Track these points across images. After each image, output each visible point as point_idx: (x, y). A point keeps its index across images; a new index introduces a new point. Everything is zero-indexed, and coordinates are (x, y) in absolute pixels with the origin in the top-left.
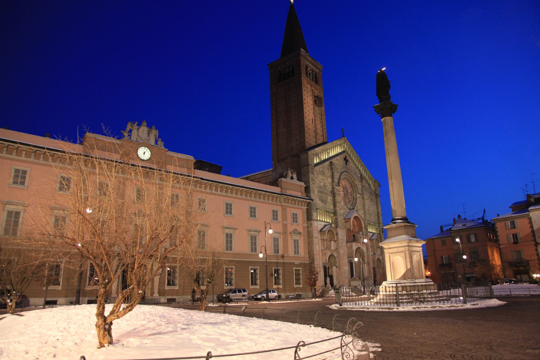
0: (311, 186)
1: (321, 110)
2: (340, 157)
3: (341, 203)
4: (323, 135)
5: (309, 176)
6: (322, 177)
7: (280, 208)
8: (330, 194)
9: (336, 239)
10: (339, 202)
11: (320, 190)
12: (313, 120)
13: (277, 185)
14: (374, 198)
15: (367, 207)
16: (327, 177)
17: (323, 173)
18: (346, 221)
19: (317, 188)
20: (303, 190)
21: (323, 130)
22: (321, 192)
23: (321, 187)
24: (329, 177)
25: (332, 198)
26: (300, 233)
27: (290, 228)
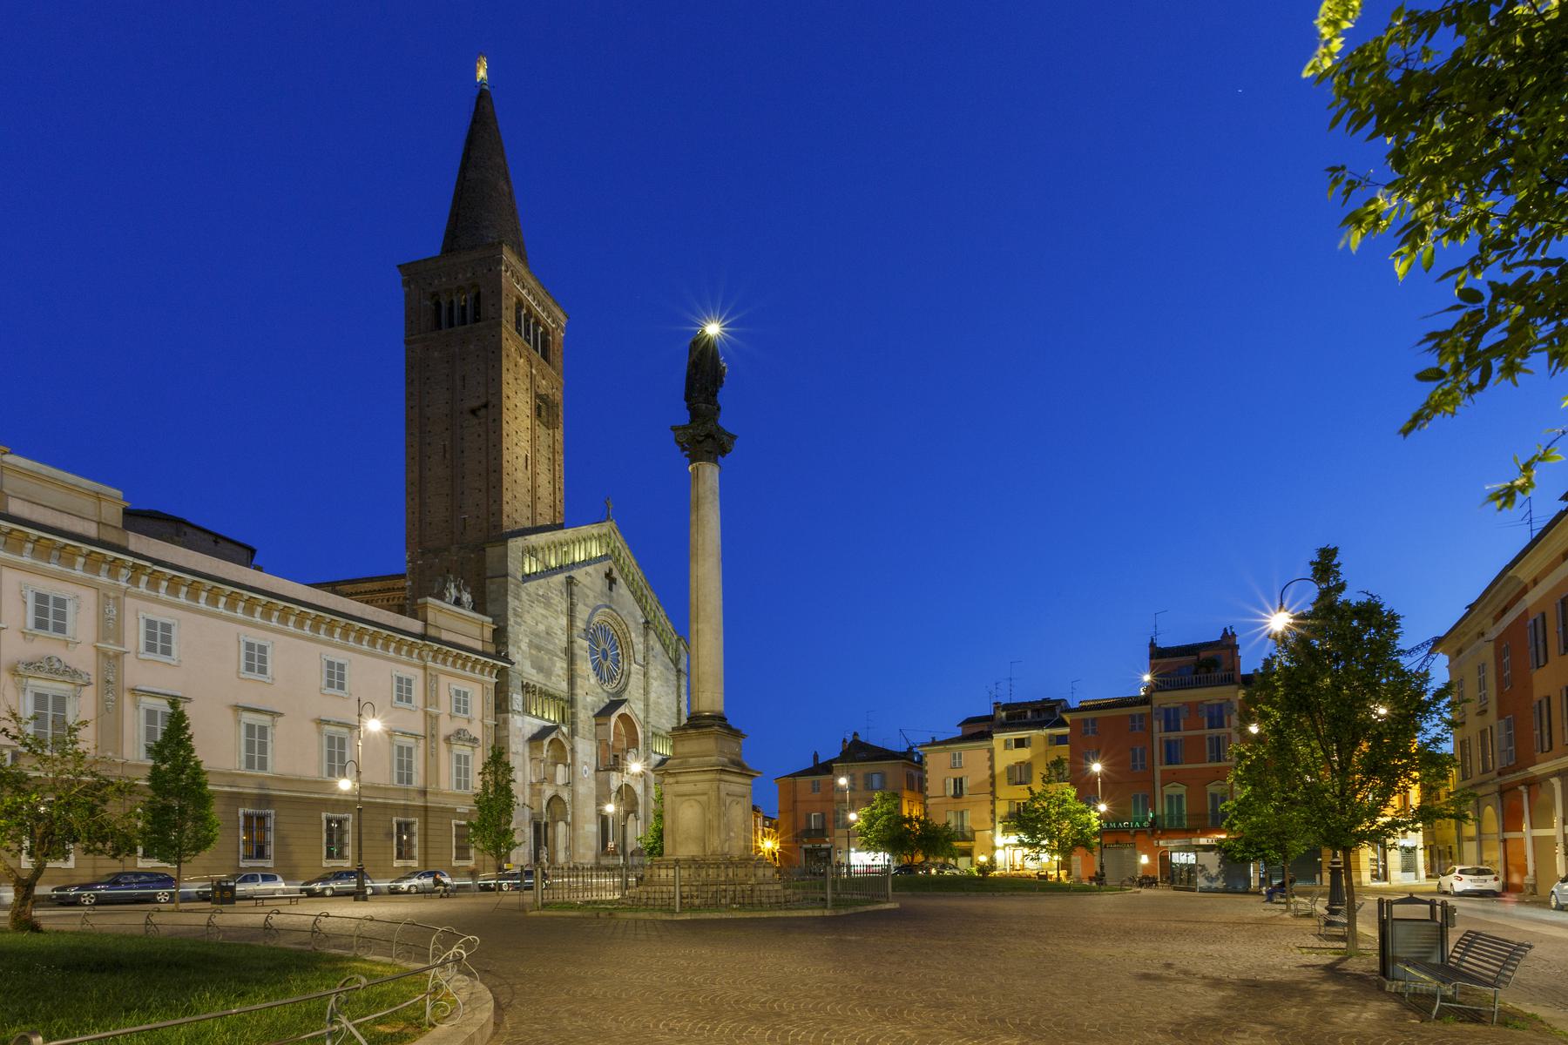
0: (509, 628)
2: (595, 569)
5: (507, 603)
6: (544, 612)
7: (420, 673)
8: (563, 655)
9: (569, 761)
10: (583, 677)
11: (536, 641)
14: (673, 677)
15: (653, 696)
16: (556, 611)
17: (548, 604)
18: (599, 722)
19: (526, 635)
20: (488, 634)
22: (539, 648)
23: (537, 635)
24: (562, 612)
25: (565, 666)
26: (475, 740)
27: (446, 727)
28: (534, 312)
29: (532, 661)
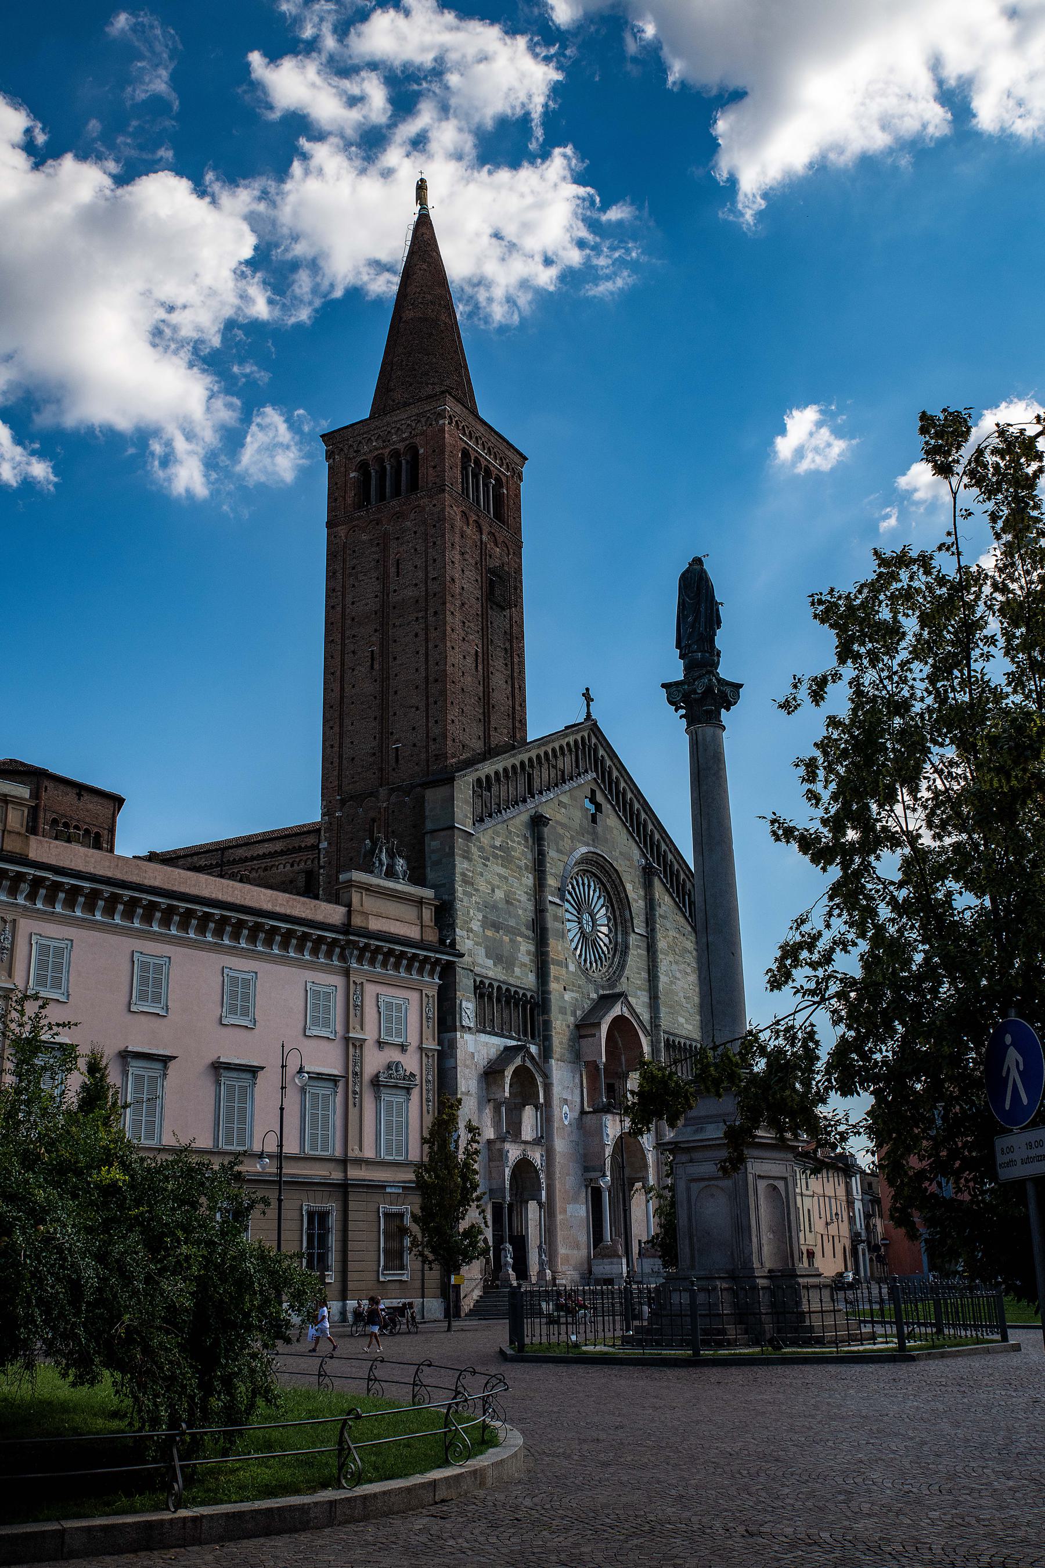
0: (458, 905)
1: (511, 619)
3: (567, 967)
4: (514, 713)
5: (454, 866)
7: (338, 980)
8: (530, 933)
9: (542, 1101)
10: (559, 963)
12: (480, 655)
13: (335, 898)
16: (520, 867)
17: (507, 860)
19: (479, 910)
21: (513, 696)
22: (496, 926)
23: (494, 907)
25: (532, 948)
27: (374, 1062)
28: (484, 463)
29: (487, 948)
